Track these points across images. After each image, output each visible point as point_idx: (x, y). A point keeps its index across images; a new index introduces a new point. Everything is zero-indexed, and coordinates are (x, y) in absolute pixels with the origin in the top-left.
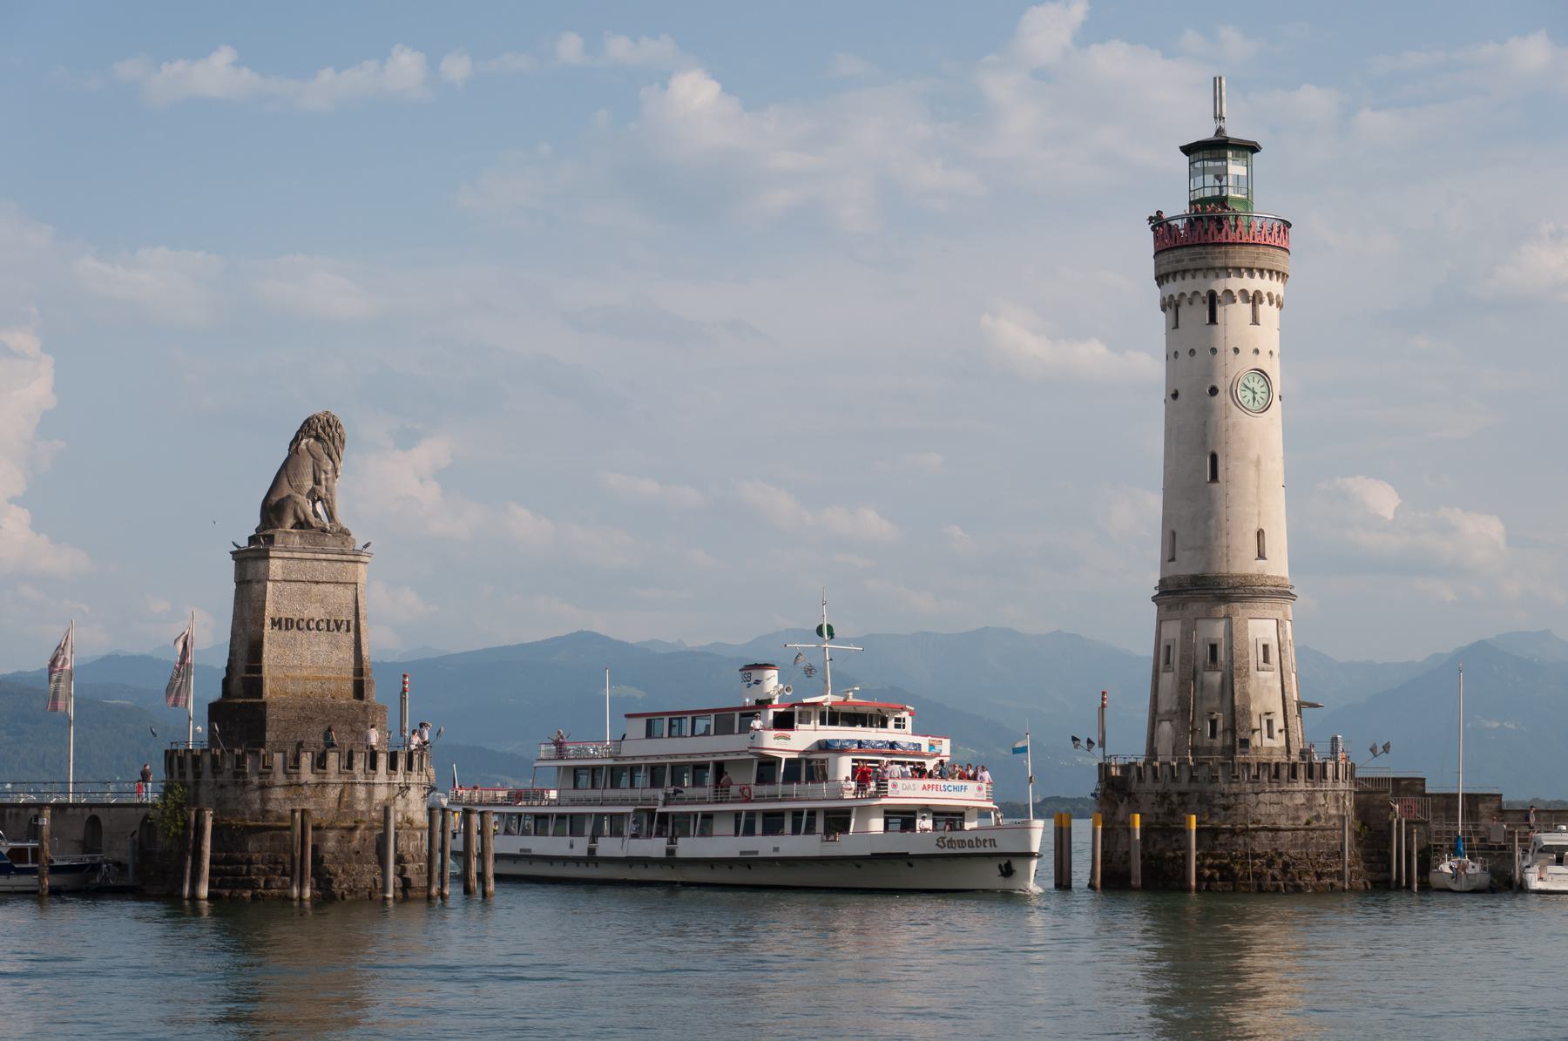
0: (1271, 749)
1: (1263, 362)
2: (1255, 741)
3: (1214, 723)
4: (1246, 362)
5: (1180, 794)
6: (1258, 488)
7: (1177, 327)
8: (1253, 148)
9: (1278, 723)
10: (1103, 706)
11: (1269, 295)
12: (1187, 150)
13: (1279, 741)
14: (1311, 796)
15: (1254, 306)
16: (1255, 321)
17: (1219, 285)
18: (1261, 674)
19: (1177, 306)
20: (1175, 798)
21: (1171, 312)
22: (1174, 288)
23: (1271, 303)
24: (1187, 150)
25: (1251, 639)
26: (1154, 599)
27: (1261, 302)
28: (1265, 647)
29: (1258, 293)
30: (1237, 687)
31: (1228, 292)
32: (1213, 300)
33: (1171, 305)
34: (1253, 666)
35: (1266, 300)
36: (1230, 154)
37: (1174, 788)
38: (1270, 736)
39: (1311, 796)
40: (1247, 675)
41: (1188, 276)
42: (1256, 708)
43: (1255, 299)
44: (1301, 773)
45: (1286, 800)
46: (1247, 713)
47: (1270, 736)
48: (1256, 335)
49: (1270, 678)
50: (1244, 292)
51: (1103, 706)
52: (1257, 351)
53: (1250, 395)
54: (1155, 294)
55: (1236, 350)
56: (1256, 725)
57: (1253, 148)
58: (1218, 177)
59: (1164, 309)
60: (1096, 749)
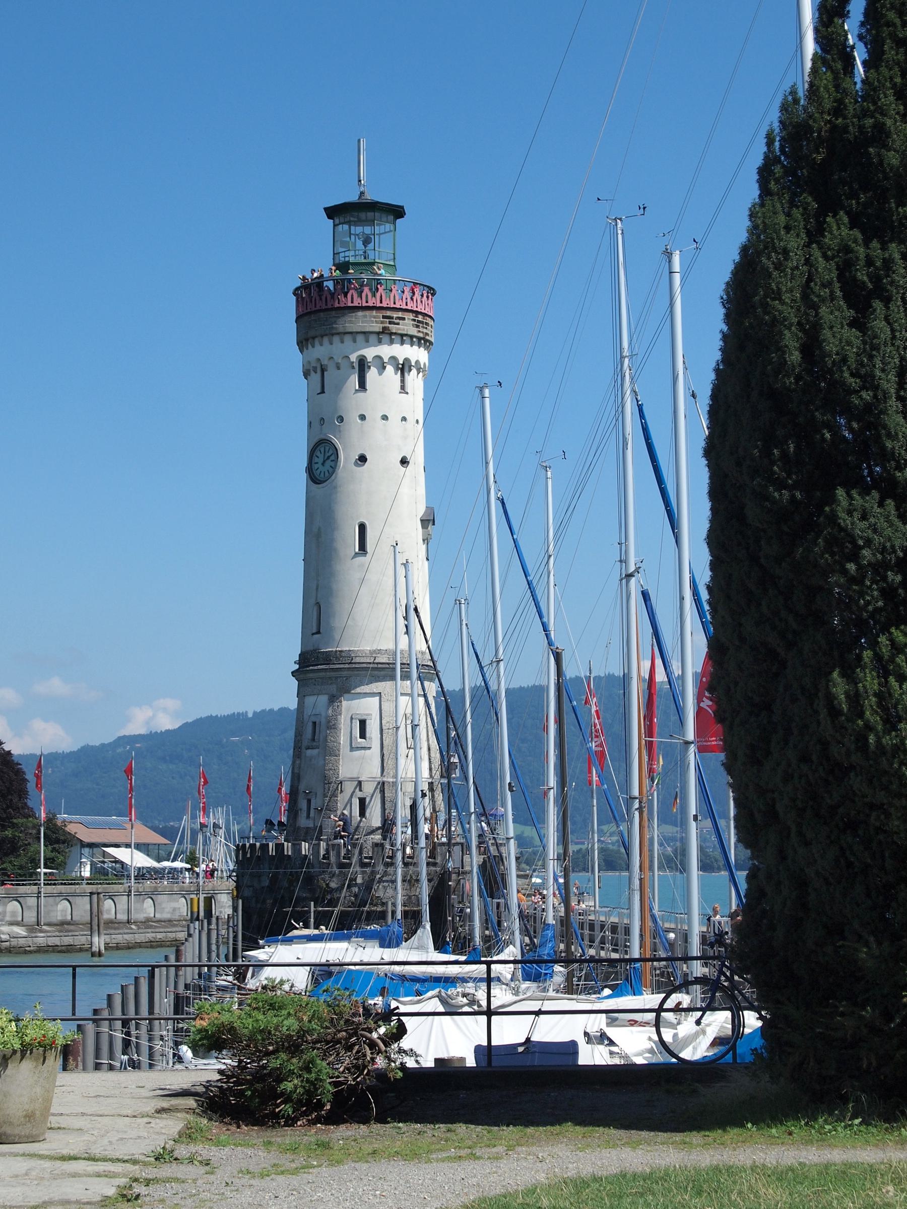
7: (323, 392)
8: (397, 212)
11: (417, 362)
12: (332, 212)
16: (403, 387)
17: (370, 353)
19: (323, 371)
21: (316, 377)
22: (320, 351)
27: (410, 370)
29: (407, 360)
31: (378, 357)
32: (363, 366)
33: (317, 372)
43: (403, 368)
50: (393, 359)
52: (404, 419)
58: (367, 241)
59: (306, 374)
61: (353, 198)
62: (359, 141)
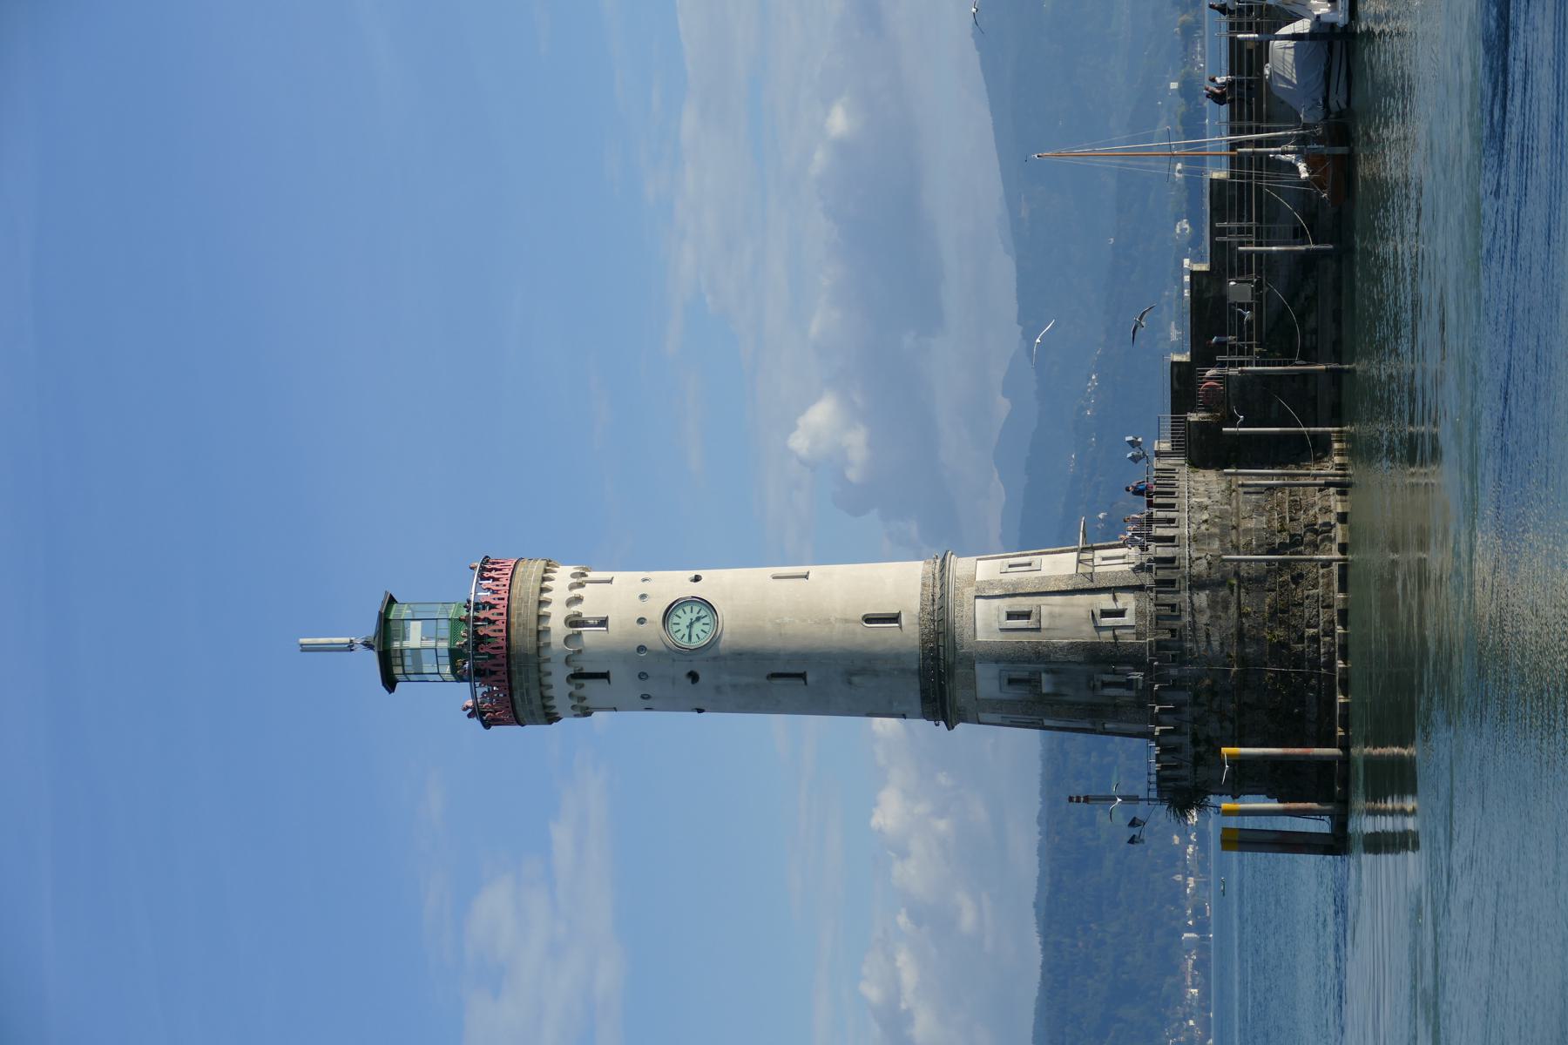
0: (1140, 614)
1: (655, 611)
2: (1129, 638)
3: (1105, 685)
4: (653, 634)
5: (1195, 742)
9: (1105, 601)
10: (1087, 799)
11: (570, 602)
13: (1127, 601)
14: (1197, 584)
15: (584, 624)
16: (603, 622)
18: (1044, 624)
20: (1202, 749)
23: (579, 599)
24: (390, 683)
25: (999, 638)
26: (950, 727)
27: (579, 615)
28: (1010, 616)
30: (1060, 656)
31: (568, 661)
32: (579, 676)
33: (587, 712)
34: (1034, 637)
35: (575, 609)
36: (396, 645)
37: (1189, 751)
38: (1121, 613)
39: (1197, 584)
41: (546, 680)
42: (1087, 634)
43: (575, 622)
44: (1166, 598)
45: (1203, 619)
47: (1121, 613)
48: (621, 599)
49: (1049, 607)
50: (567, 640)
51: (1087, 799)
52: (641, 621)
53: (697, 627)
54: (569, 725)
56: (1106, 636)
57: (392, 600)
60: (1140, 810)
61: (373, 656)
62: (305, 649)
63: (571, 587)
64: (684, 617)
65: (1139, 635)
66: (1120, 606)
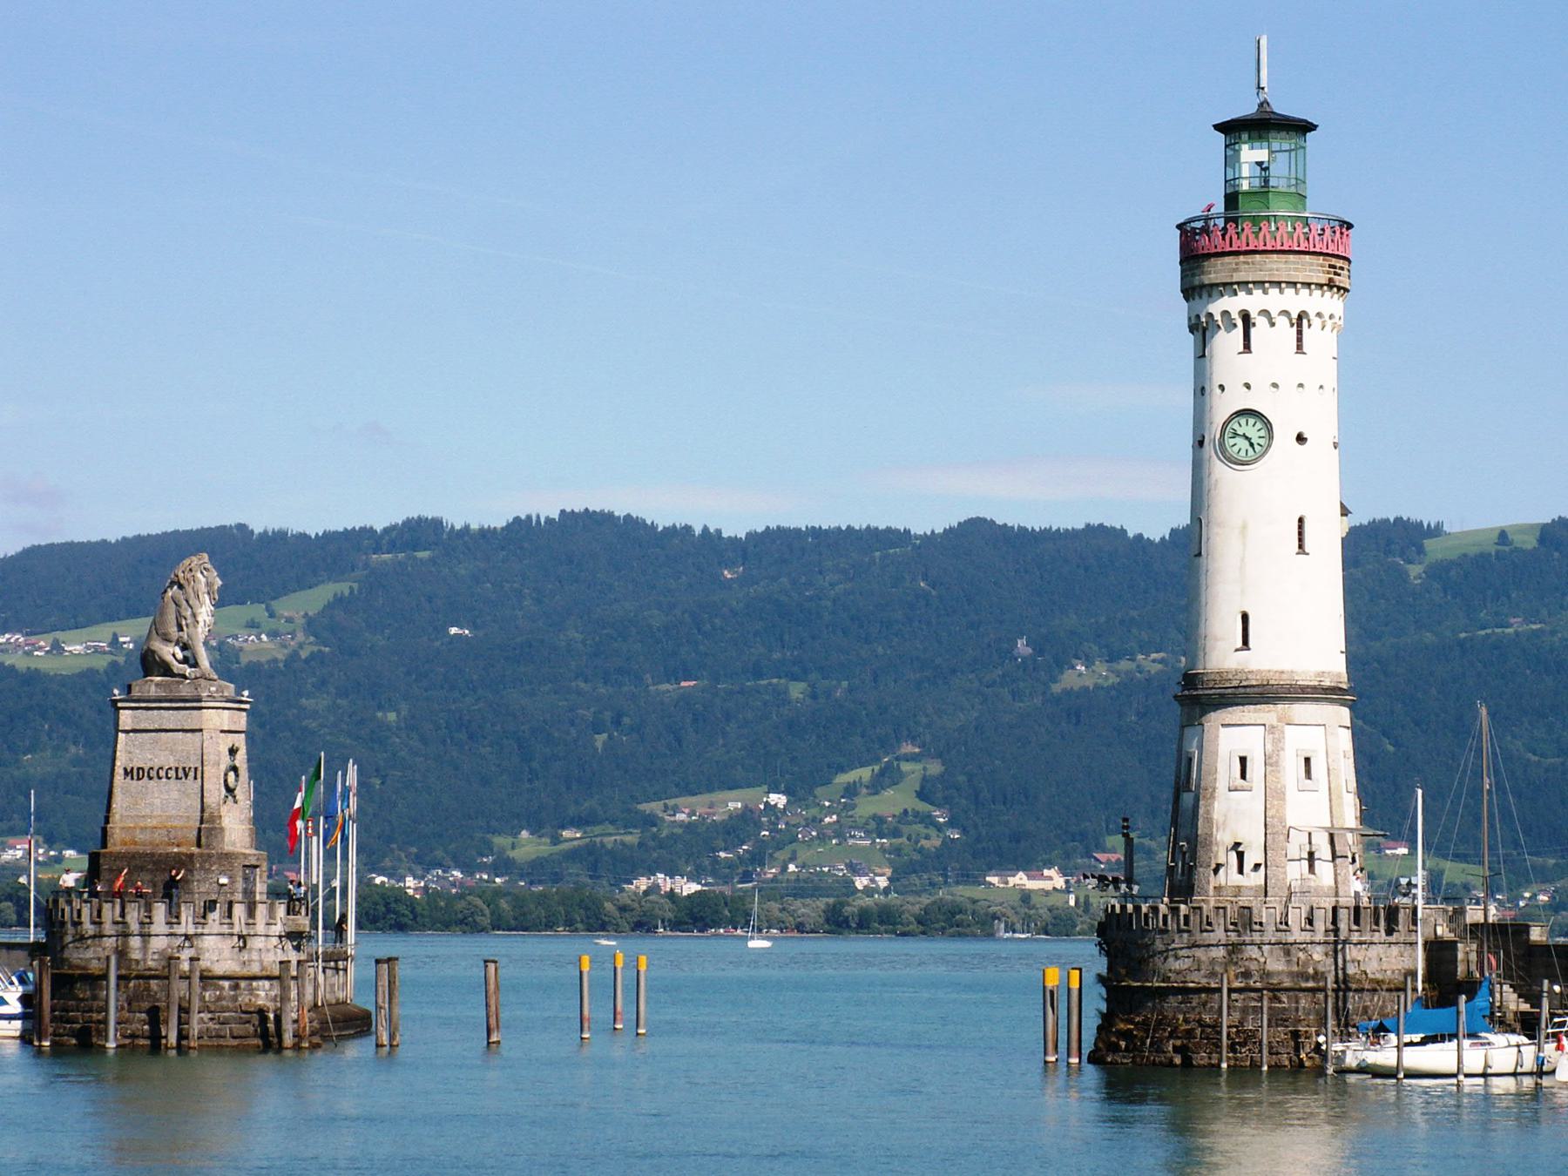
6: (1243, 560)
13: (1257, 879)
16: (1247, 347)
28: (1243, 760)
30: (1201, 811)
34: (1221, 786)
38: (1241, 871)
40: (1212, 796)
42: (1223, 838)
46: (1209, 842)
47: (1241, 871)
50: (1225, 313)
52: (1248, 386)
53: (1244, 444)
55: (1222, 387)
63: (1285, 313)
64: (1251, 428)
65: (1218, 889)
66: (1248, 866)
